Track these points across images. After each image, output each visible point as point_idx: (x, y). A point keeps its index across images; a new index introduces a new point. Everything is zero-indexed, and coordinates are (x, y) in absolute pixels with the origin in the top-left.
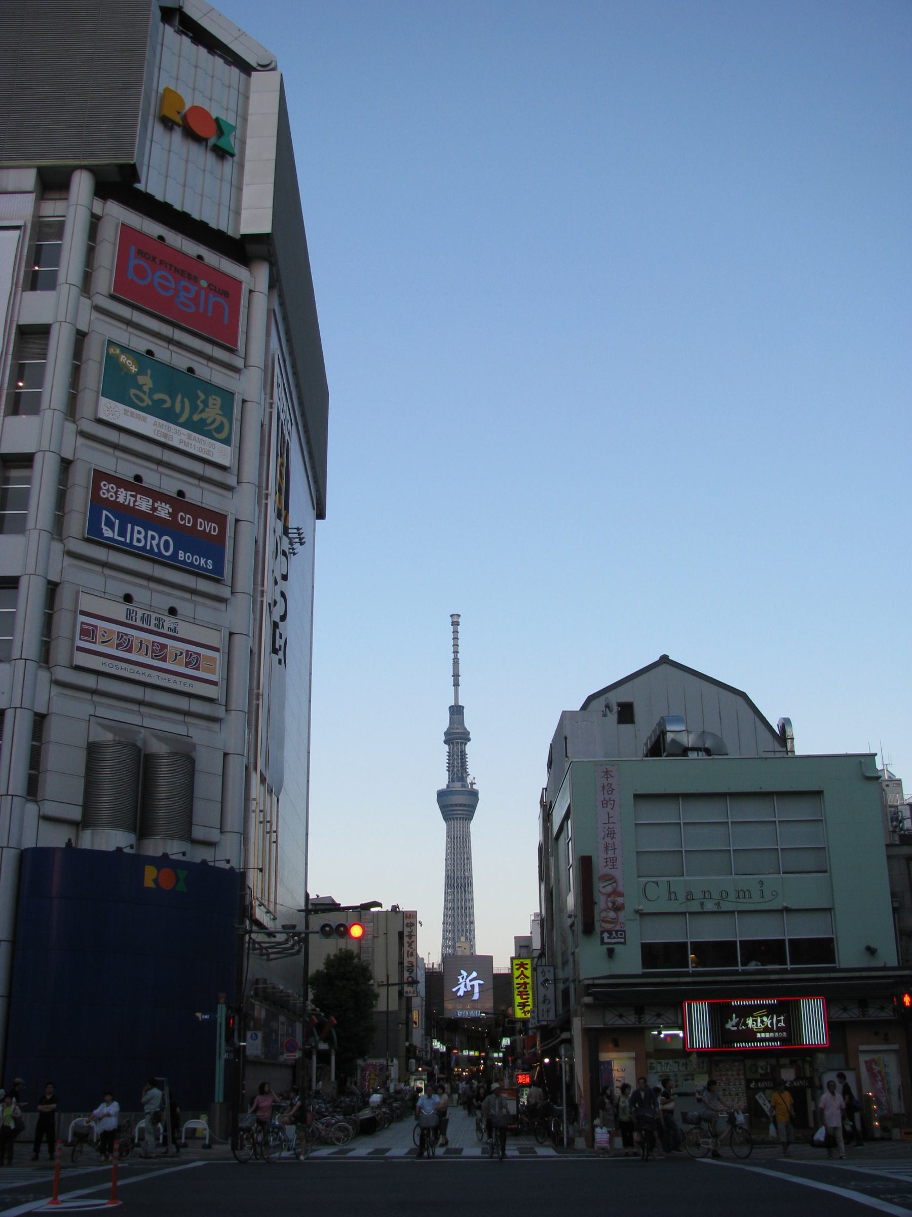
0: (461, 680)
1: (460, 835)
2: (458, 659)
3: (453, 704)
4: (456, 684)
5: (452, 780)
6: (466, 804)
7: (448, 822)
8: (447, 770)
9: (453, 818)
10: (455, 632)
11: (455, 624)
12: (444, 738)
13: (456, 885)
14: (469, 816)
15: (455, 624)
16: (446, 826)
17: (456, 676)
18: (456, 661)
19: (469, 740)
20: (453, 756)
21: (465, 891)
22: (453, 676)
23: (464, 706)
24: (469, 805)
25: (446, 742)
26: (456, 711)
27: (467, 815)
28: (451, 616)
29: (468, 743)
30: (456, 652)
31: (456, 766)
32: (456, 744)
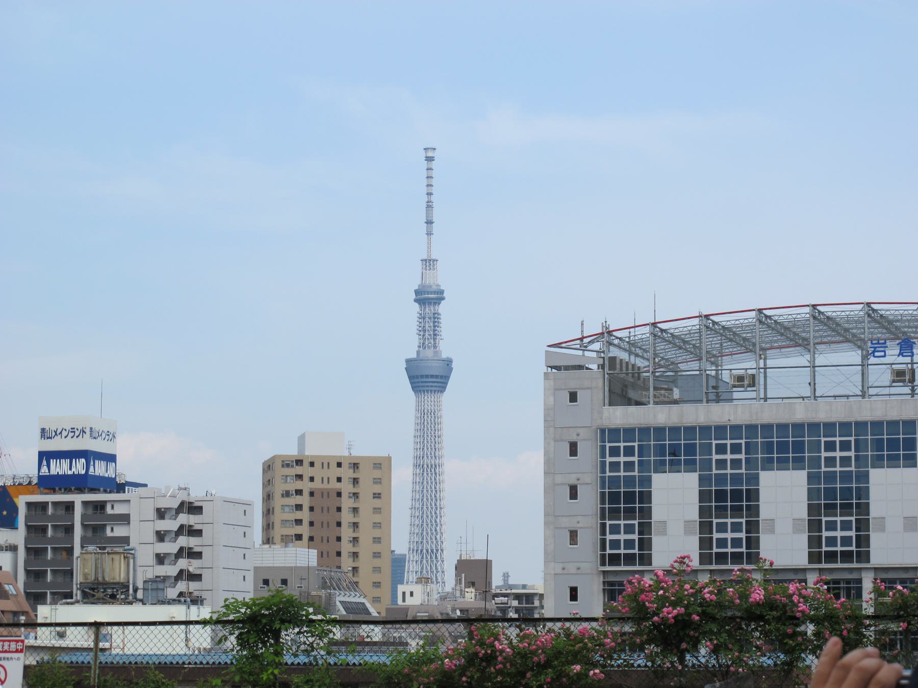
4: (429, 234)
5: (423, 346)
6: (438, 376)
9: (424, 391)
10: (429, 169)
11: (429, 159)
12: (414, 296)
15: (429, 159)
16: (415, 397)
17: (429, 222)
18: (429, 206)
19: (443, 299)
20: (424, 318)
22: (426, 222)
24: (442, 377)
25: (416, 301)
26: (429, 263)
27: (439, 387)
29: (443, 302)
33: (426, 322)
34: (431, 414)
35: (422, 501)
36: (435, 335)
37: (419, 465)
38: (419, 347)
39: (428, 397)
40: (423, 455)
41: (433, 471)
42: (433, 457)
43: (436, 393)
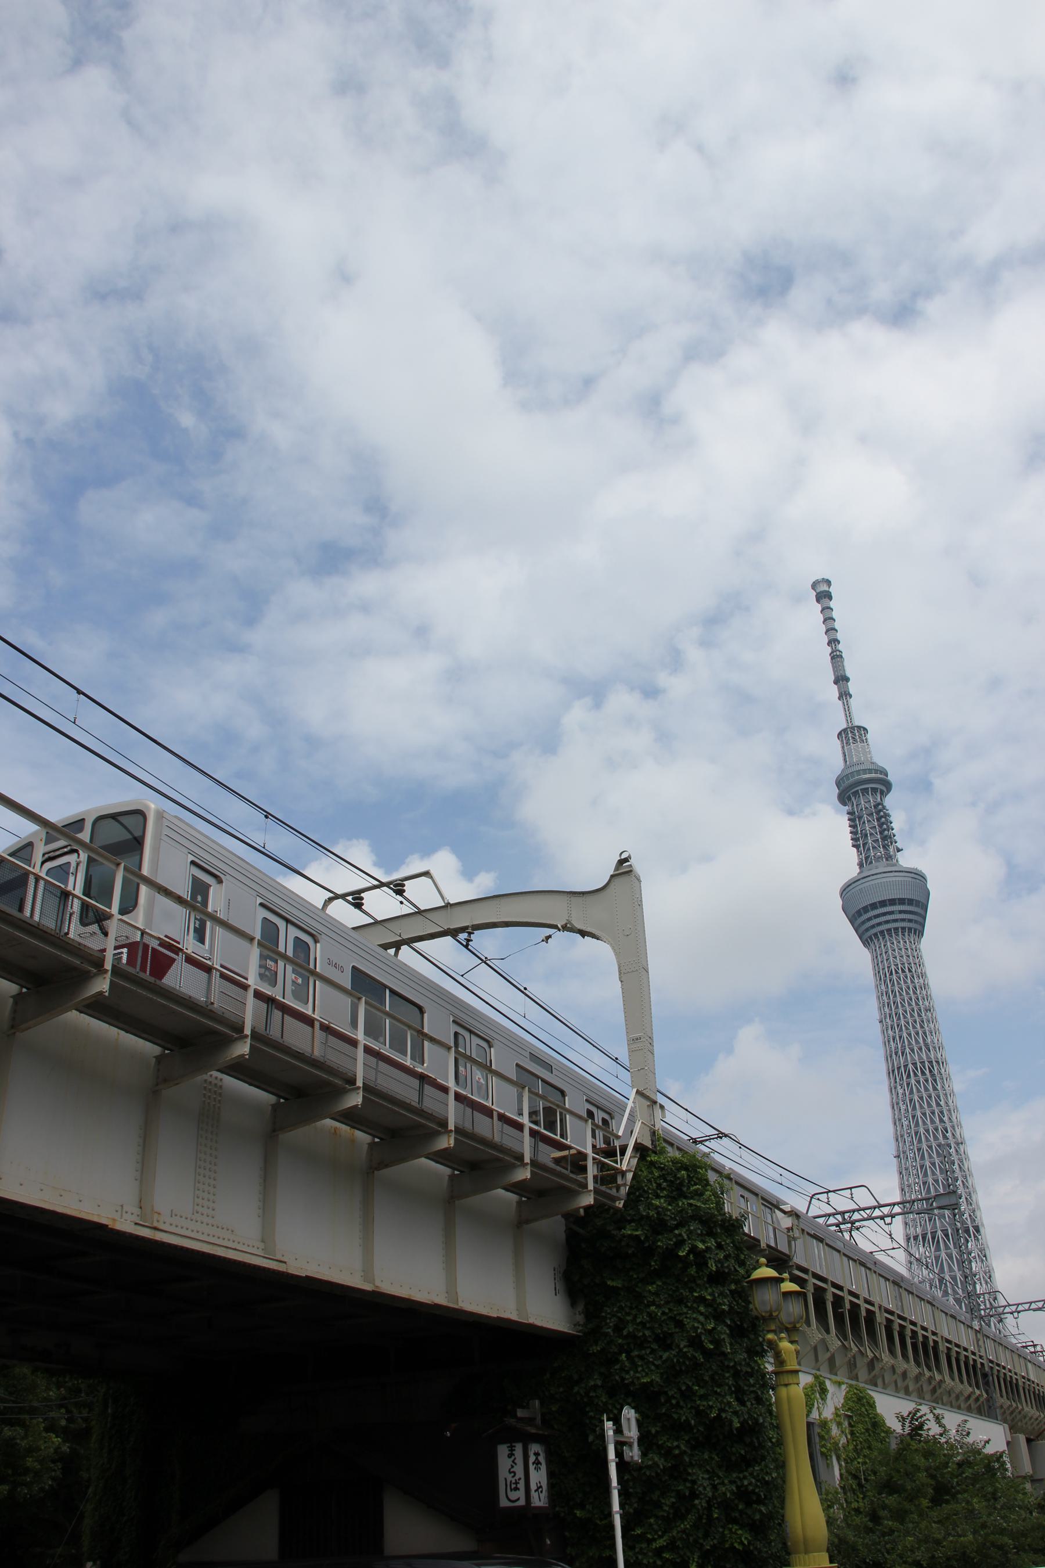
0: (852, 687)
1: (903, 964)
2: (840, 651)
3: (844, 725)
4: (844, 695)
6: (904, 899)
7: (872, 945)
8: (853, 846)
10: (826, 609)
11: (823, 596)
13: (910, 1066)
14: (917, 929)
15: (823, 596)
20: (860, 818)
21: (933, 1075)
23: (866, 727)
28: (814, 586)
30: (833, 642)
31: (871, 834)
32: (863, 795)
33: (864, 822)
34: (903, 971)
35: (916, 1135)
36: (884, 838)
37: (899, 1068)
38: (861, 865)
39: (893, 943)
40: (902, 1046)
41: (927, 1072)
42: (923, 1048)
43: (906, 934)
